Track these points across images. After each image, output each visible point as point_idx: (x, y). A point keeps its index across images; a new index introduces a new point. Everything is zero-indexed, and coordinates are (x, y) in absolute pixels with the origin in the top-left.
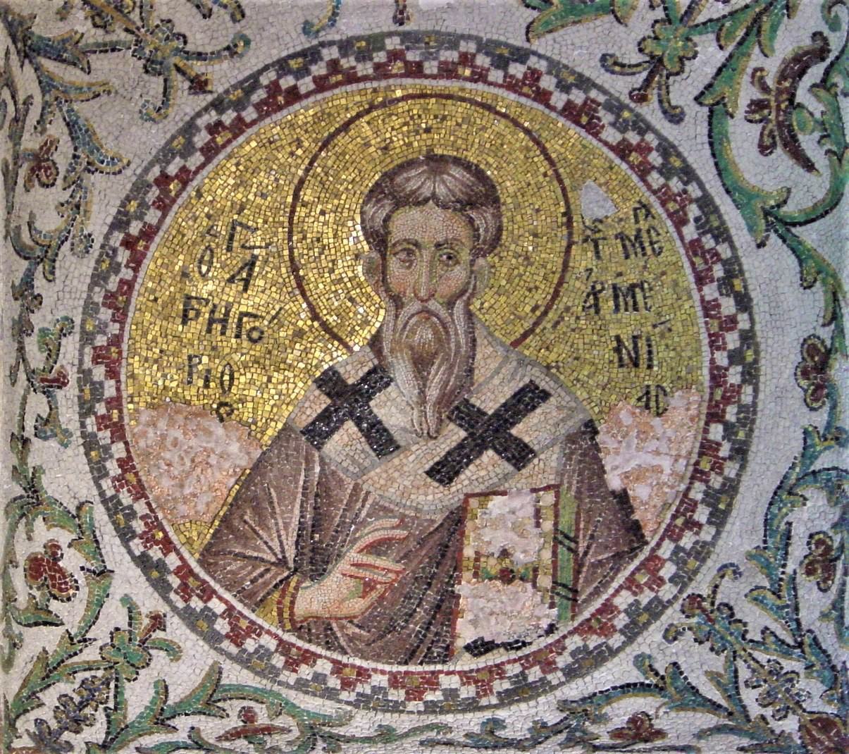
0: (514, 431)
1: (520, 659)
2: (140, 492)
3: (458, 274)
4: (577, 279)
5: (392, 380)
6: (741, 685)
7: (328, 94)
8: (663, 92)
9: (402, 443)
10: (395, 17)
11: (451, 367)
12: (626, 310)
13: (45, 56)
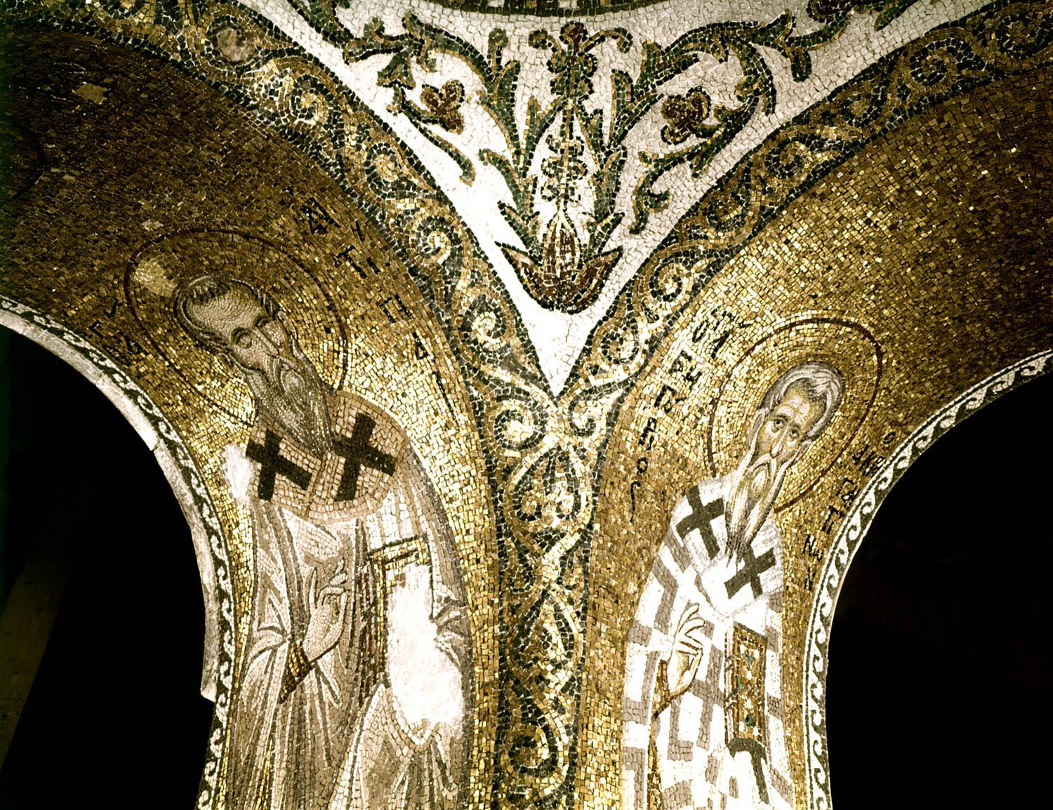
6: (545, 135)
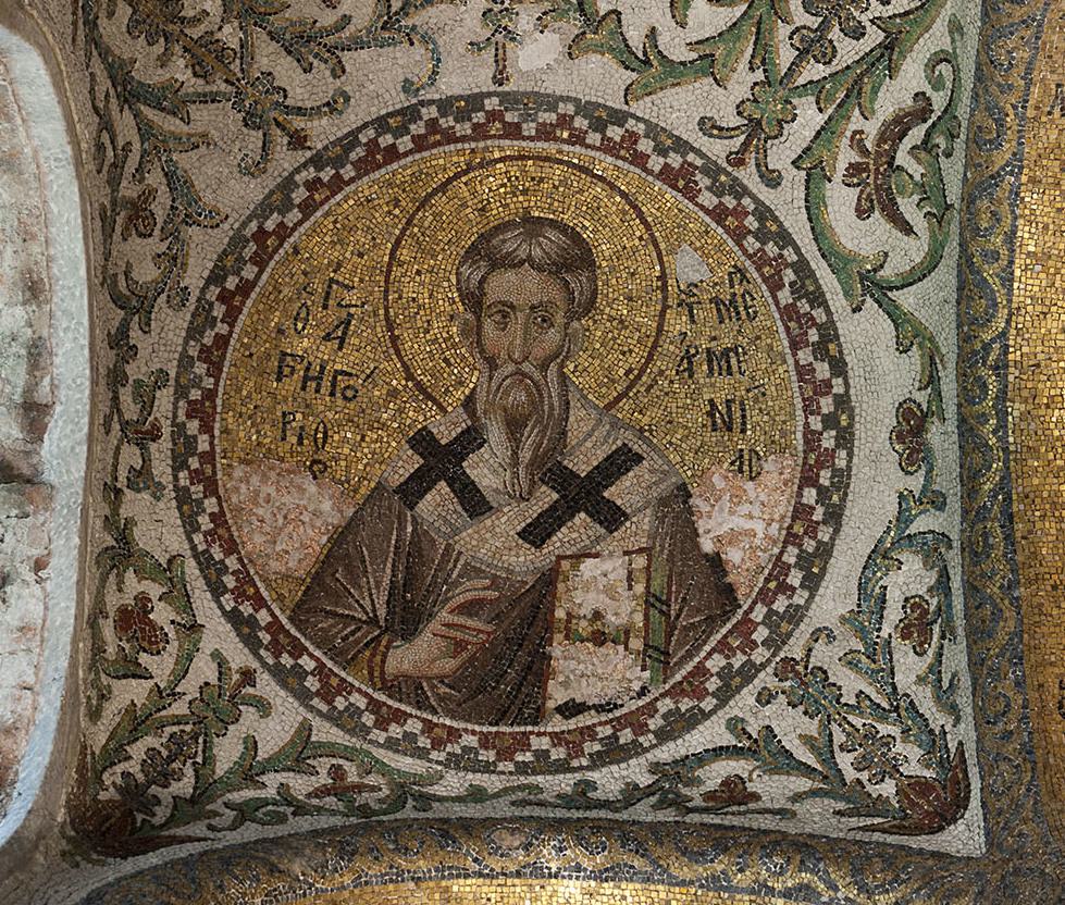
0: (606, 494)
1: (611, 721)
2: (231, 547)
3: (553, 336)
4: (671, 343)
5: (485, 441)
6: (836, 748)
7: (426, 154)
8: (761, 156)
9: (495, 505)
10: (495, 77)
11: (546, 427)
12: (720, 374)
13: (145, 104)
